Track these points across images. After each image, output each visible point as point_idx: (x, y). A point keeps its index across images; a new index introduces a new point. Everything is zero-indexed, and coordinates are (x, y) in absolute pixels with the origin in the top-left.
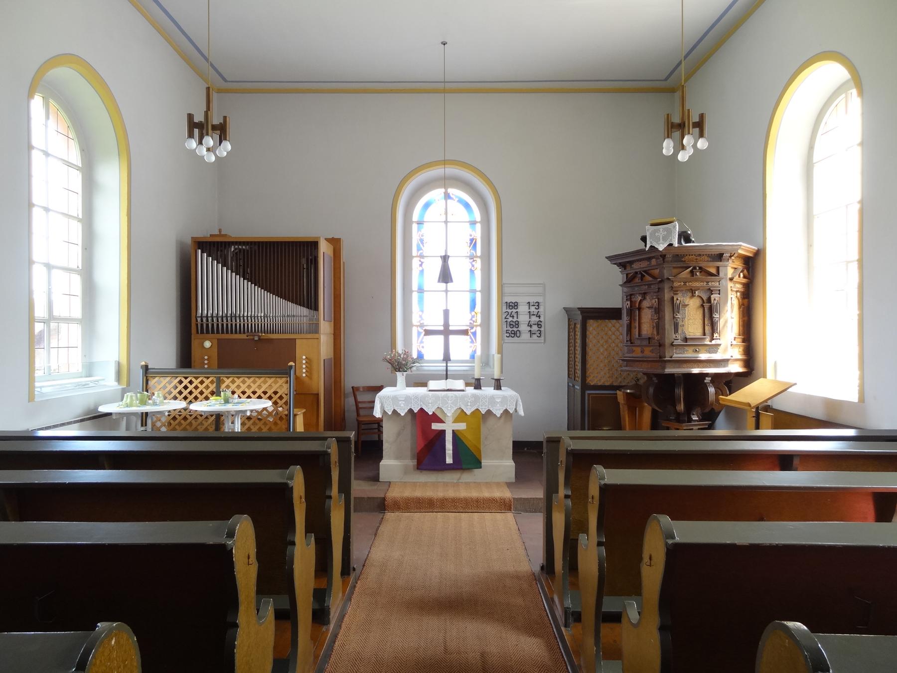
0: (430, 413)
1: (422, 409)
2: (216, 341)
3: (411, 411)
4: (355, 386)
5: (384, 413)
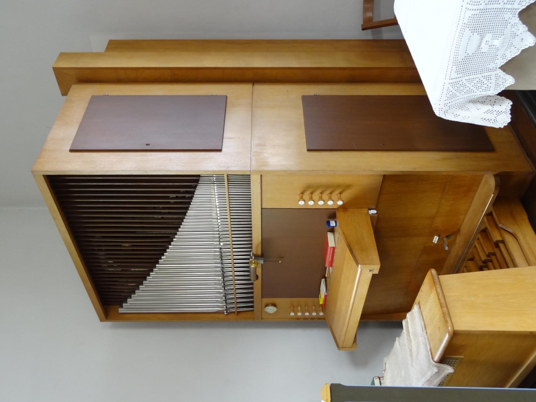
2: (266, 300)
4: (360, 22)
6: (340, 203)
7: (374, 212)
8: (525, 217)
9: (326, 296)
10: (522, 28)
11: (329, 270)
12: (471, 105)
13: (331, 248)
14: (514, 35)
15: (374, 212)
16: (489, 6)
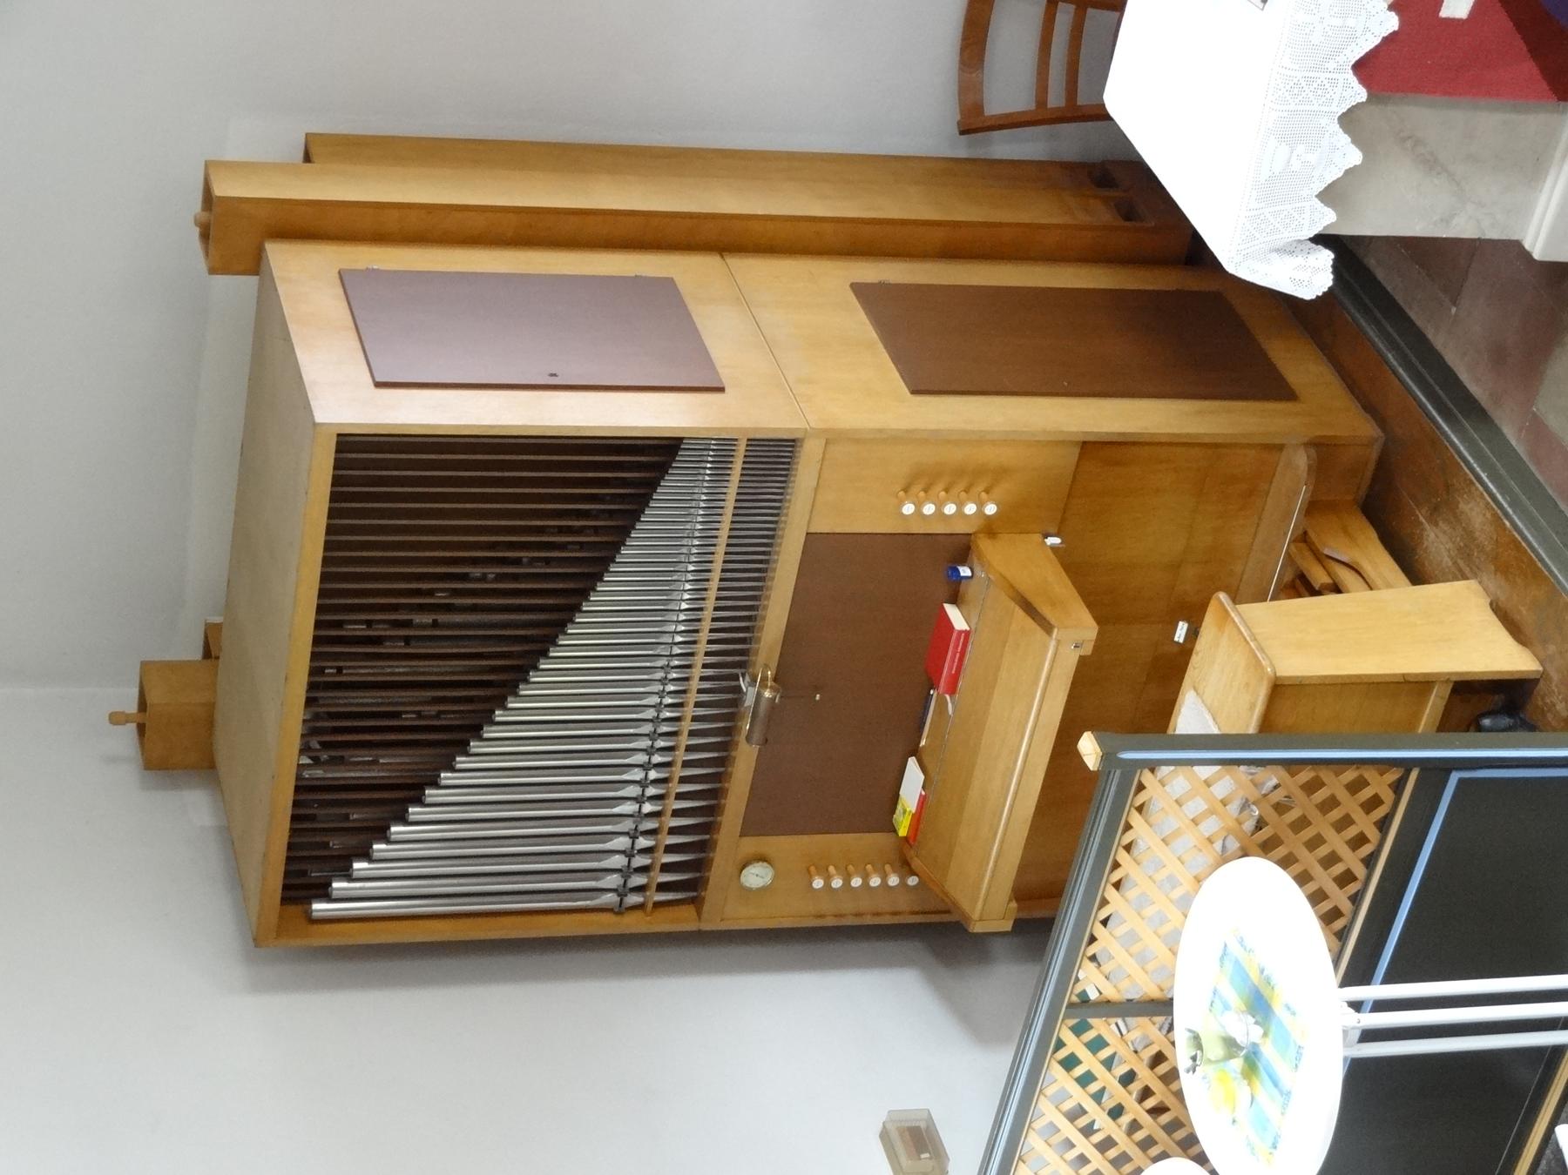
0: (1392, 23)
2: (750, 845)
3: (1349, 121)
6: (991, 509)
7: (1055, 541)
8: (1373, 535)
9: (923, 802)
10: (1345, 139)
11: (942, 705)
12: (1275, 255)
13: (960, 632)
14: (1335, 149)
15: (1055, 541)
16: (1300, 108)
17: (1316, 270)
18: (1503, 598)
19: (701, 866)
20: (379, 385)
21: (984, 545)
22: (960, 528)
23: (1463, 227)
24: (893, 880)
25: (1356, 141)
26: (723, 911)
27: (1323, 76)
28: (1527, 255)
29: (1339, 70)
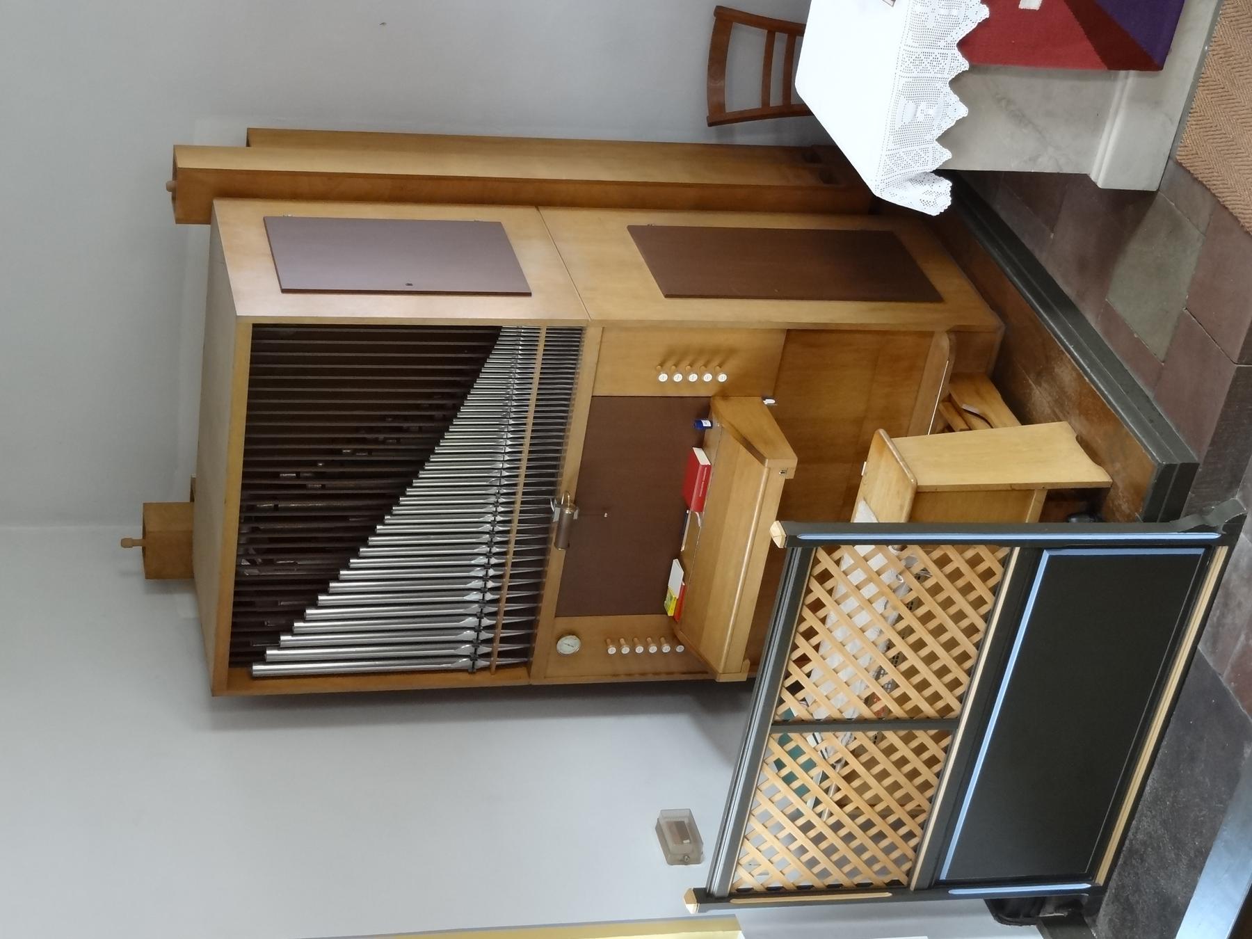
0: (984, 12)
1: (964, 45)
2: (563, 623)
3: (957, 83)
4: (703, 113)
5: (940, 173)
6: (722, 378)
7: (772, 401)
8: (998, 396)
9: (683, 589)
10: (954, 98)
11: (694, 519)
14: (948, 105)
15: (772, 401)
17: (939, 194)
18: (1084, 432)
19: (529, 639)
20: (284, 291)
21: (720, 405)
22: (703, 393)
23: (1045, 164)
24: (666, 649)
25: (964, 99)
26: (546, 672)
27: (936, 51)
28: (1095, 184)
29: (948, 47)
